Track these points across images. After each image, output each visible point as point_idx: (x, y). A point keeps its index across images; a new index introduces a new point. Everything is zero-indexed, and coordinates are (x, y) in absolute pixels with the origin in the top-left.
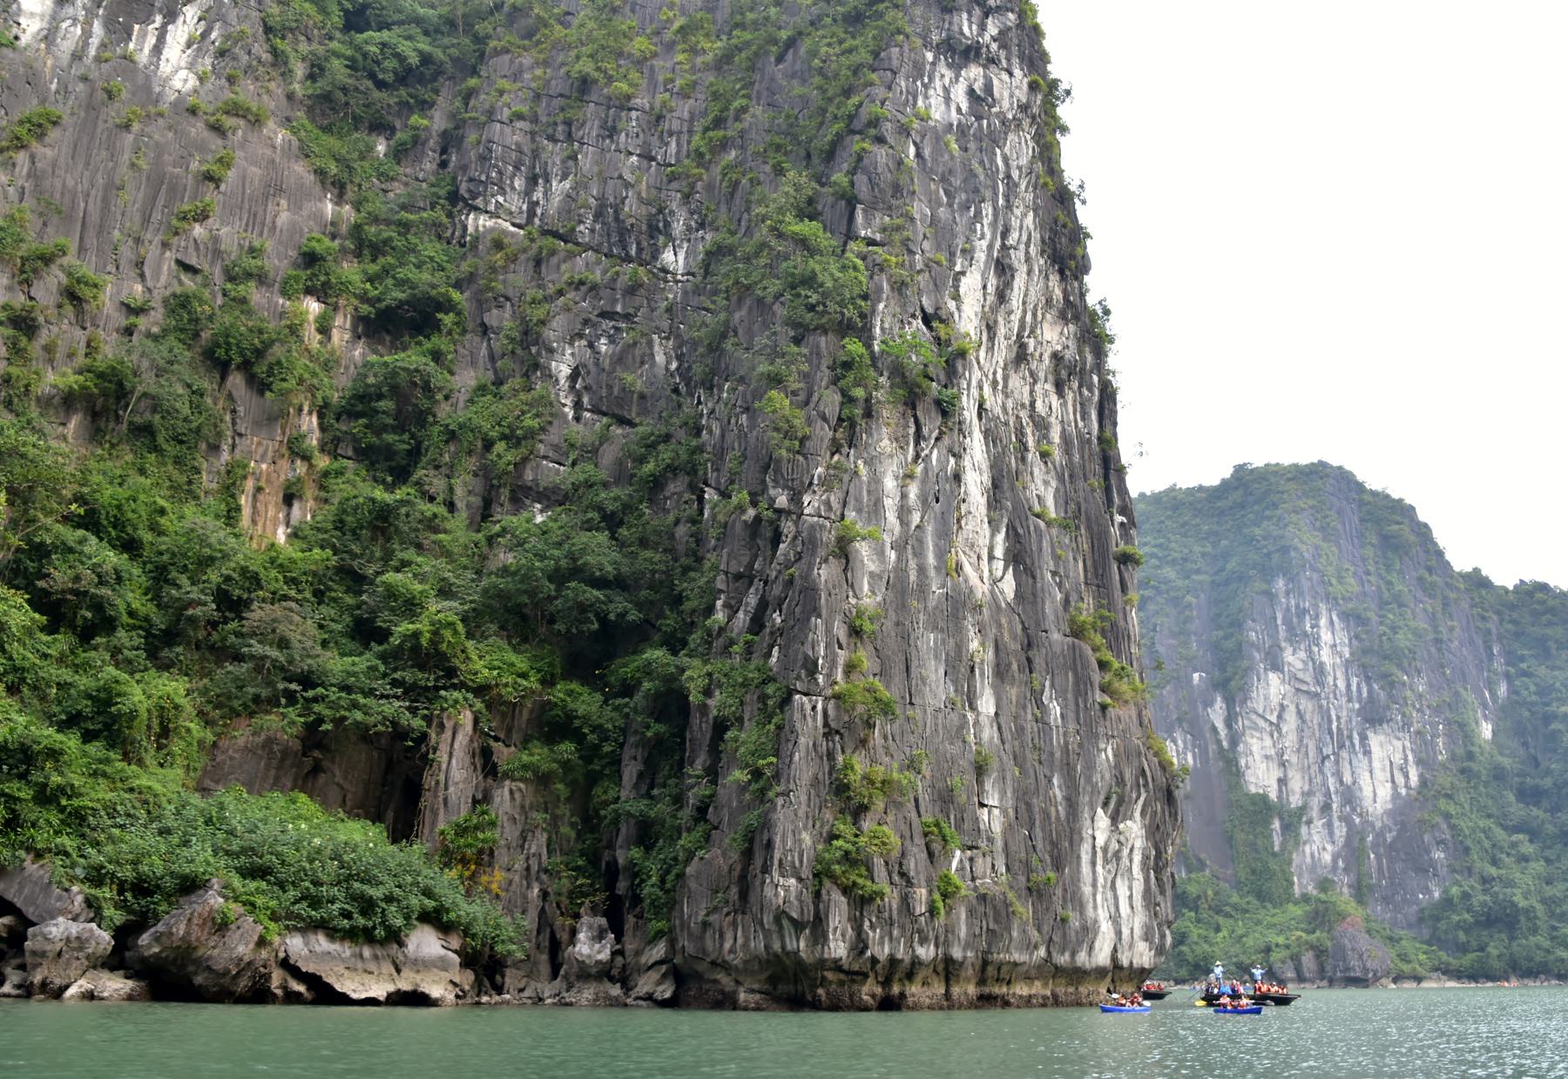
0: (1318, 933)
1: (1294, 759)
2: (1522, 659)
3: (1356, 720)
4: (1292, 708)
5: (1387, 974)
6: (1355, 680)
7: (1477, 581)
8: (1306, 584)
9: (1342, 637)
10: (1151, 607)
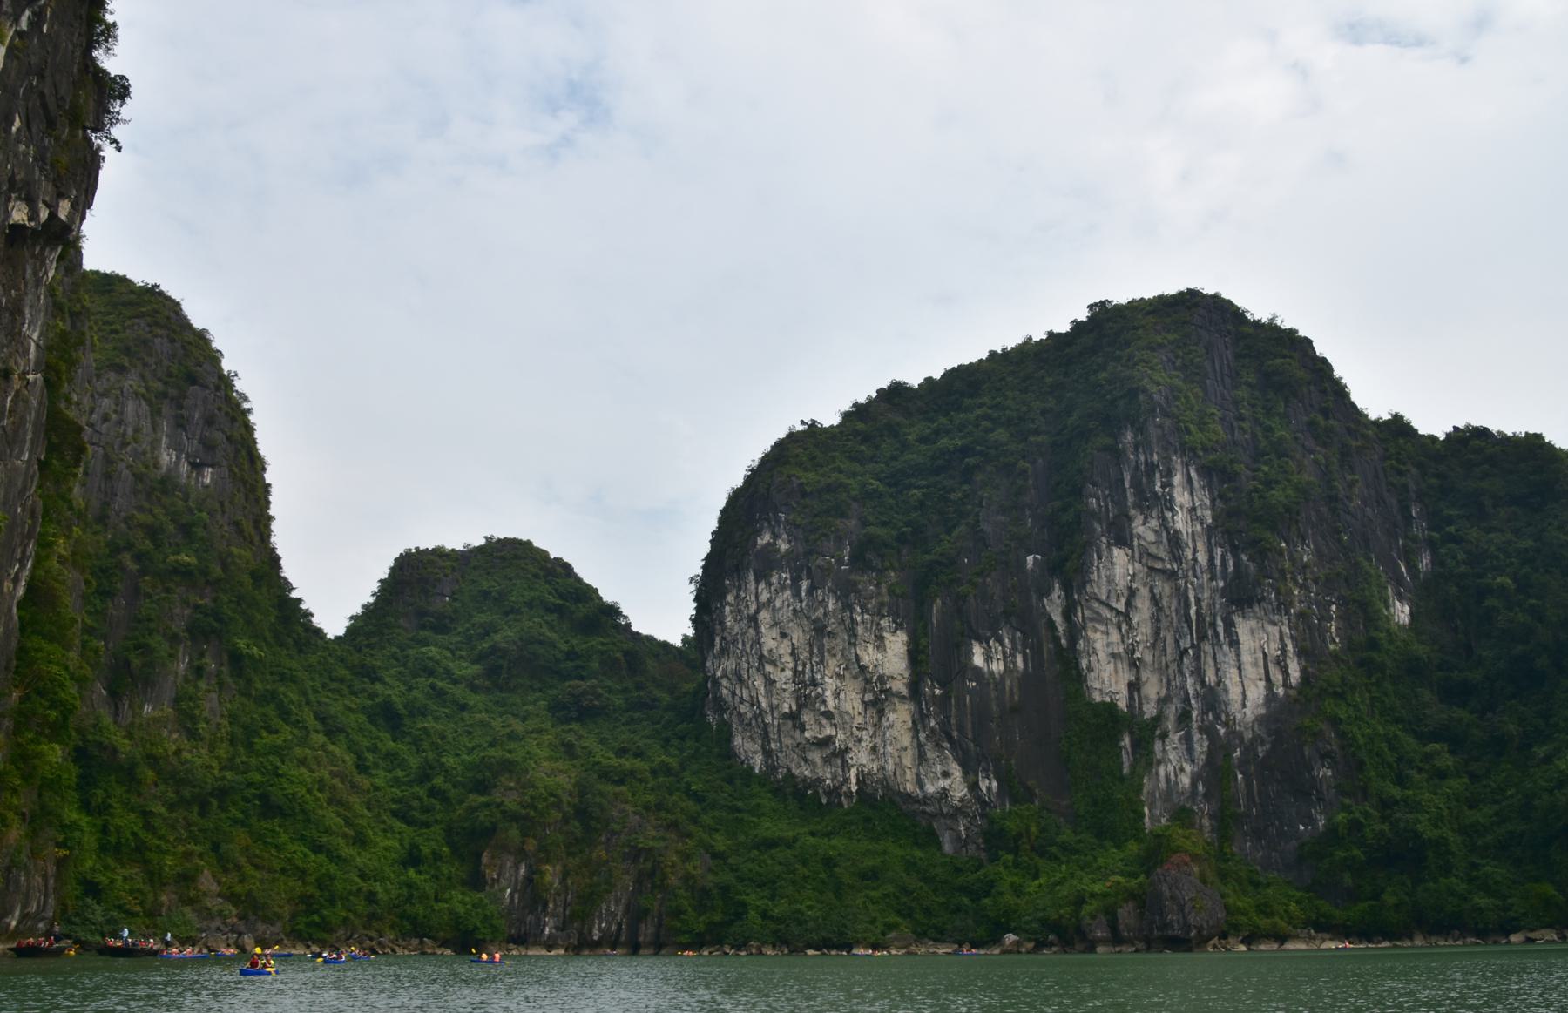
0: (1142, 878)
1: (1148, 658)
2: (1450, 522)
3: (1220, 601)
4: (1144, 591)
5: (1236, 928)
6: (1219, 551)
7: (1398, 427)
8: (1153, 433)
9: (1203, 498)
10: (979, 477)
